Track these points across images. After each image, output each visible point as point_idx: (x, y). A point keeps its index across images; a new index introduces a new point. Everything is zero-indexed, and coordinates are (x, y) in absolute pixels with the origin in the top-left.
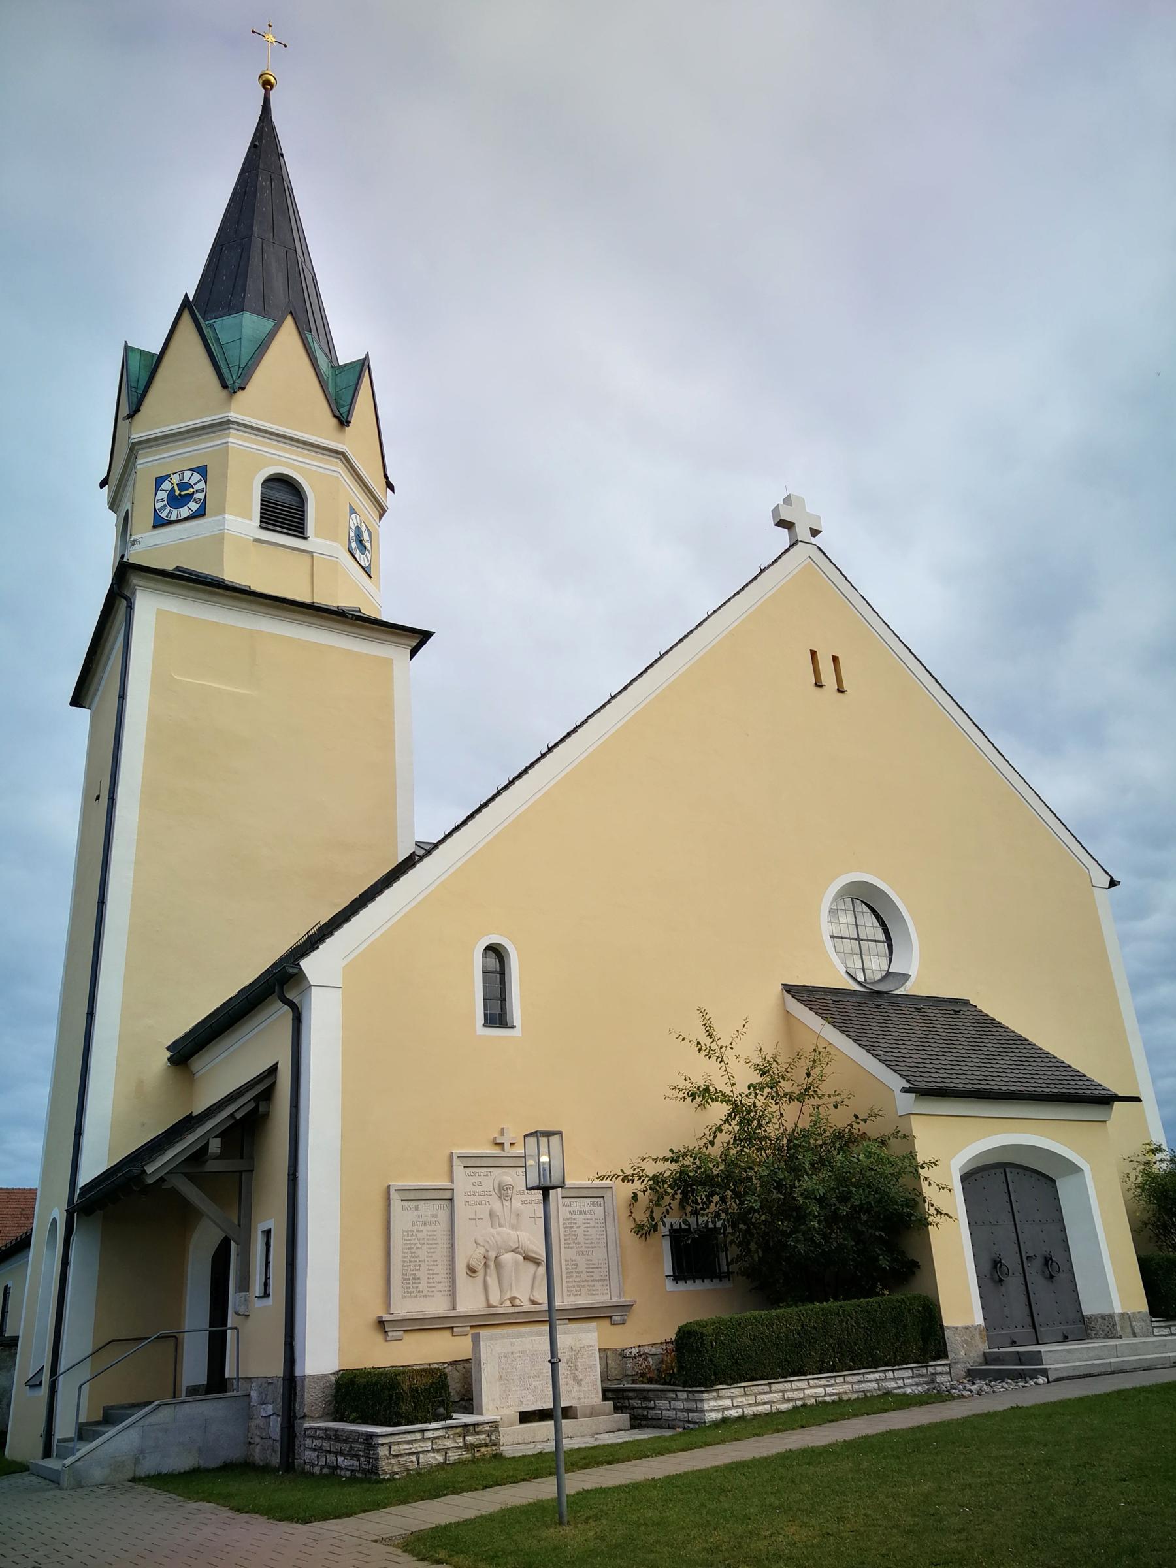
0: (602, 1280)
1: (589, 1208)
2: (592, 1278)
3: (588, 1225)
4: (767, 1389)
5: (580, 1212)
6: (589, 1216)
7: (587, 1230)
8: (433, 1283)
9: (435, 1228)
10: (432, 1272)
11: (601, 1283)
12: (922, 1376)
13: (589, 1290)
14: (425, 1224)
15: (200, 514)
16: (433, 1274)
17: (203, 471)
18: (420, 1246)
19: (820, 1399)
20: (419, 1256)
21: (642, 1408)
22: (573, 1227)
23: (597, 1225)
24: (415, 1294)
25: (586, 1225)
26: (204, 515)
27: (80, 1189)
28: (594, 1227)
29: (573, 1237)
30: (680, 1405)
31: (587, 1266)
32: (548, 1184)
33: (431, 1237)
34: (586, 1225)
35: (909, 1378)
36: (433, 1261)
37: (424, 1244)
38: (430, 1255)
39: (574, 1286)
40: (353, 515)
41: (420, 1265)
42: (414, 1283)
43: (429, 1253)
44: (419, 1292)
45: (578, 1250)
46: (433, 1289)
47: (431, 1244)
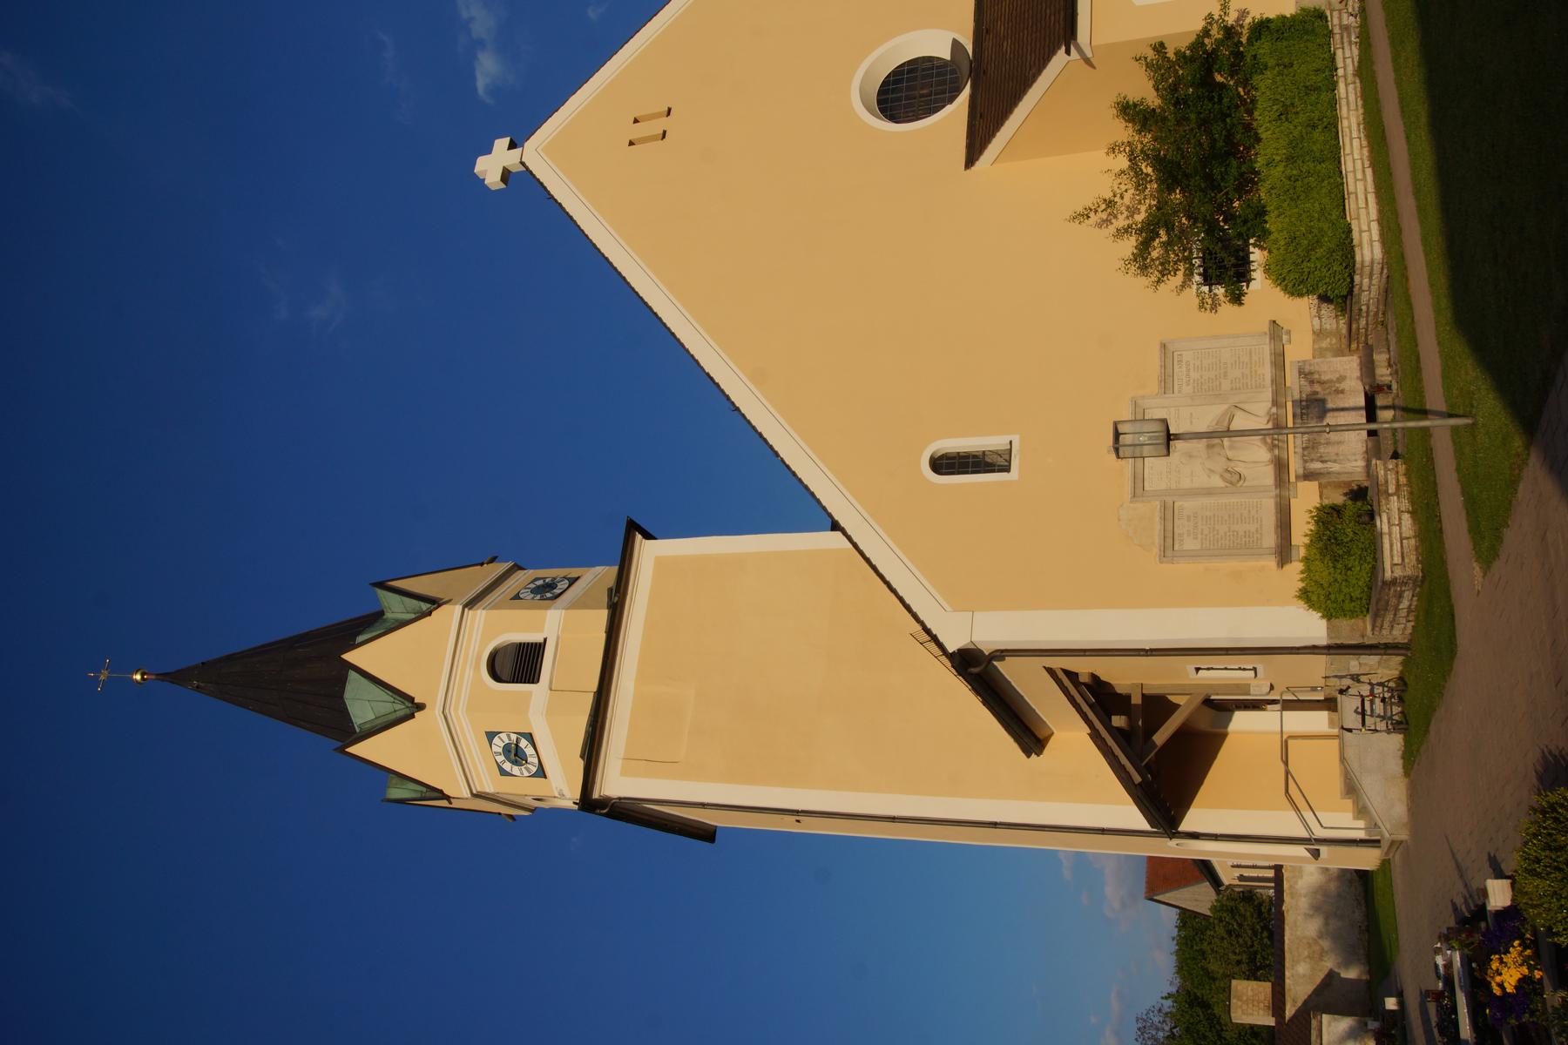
4: (1353, 196)
8: (1249, 518)
11: (1253, 355)
12: (1342, 38)
14: (1196, 527)
15: (530, 737)
17: (491, 736)
18: (1216, 532)
19: (1363, 142)
20: (1225, 533)
21: (1367, 316)
24: (1259, 536)
26: (531, 734)
27: (1152, 827)
30: (1366, 281)
32: (1163, 434)
35: (1344, 53)
40: (521, 596)
41: (1233, 532)
42: (1249, 536)
44: (1257, 531)
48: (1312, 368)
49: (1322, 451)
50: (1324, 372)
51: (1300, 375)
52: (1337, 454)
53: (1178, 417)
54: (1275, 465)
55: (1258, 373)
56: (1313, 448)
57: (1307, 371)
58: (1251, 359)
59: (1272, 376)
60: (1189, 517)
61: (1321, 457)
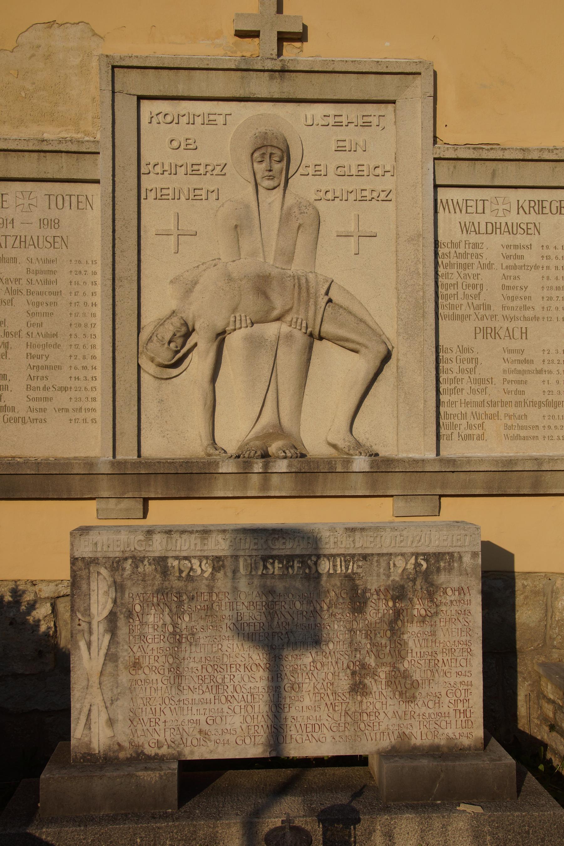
0: (548, 404)
1: (523, 218)
2: (520, 398)
3: (518, 262)
5: (495, 228)
6: (524, 240)
7: (512, 273)
8: (45, 388)
9: (51, 253)
10: (40, 362)
11: (545, 411)
13: (511, 427)
14: (22, 242)
16: (47, 367)
22: (466, 266)
23: (545, 263)
25: (511, 262)
28: (536, 267)
29: (470, 292)
31: (506, 366)
33: (40, 277)
34: (511, 262)
36: (47, 335)
37: (19, 292)
38: (35, 320)
39: (464, 416)
43: (33, 315)
45: (481, 324)
46: (43, 405)
47: (39, 293)
48: (451, 596)
49: (151, 619)
50: (433, 634)
51: (427, 556)
52: (136, 665)
53: (363, 199)
54: (187, 463)
55: (488, 424)
56: (161, 591)
57: (442, 579)
58: (533, 404)
59: (469, 461)
60: (55, 223)
61: (130, 615)
